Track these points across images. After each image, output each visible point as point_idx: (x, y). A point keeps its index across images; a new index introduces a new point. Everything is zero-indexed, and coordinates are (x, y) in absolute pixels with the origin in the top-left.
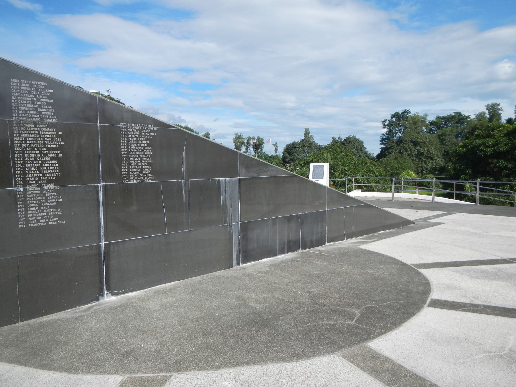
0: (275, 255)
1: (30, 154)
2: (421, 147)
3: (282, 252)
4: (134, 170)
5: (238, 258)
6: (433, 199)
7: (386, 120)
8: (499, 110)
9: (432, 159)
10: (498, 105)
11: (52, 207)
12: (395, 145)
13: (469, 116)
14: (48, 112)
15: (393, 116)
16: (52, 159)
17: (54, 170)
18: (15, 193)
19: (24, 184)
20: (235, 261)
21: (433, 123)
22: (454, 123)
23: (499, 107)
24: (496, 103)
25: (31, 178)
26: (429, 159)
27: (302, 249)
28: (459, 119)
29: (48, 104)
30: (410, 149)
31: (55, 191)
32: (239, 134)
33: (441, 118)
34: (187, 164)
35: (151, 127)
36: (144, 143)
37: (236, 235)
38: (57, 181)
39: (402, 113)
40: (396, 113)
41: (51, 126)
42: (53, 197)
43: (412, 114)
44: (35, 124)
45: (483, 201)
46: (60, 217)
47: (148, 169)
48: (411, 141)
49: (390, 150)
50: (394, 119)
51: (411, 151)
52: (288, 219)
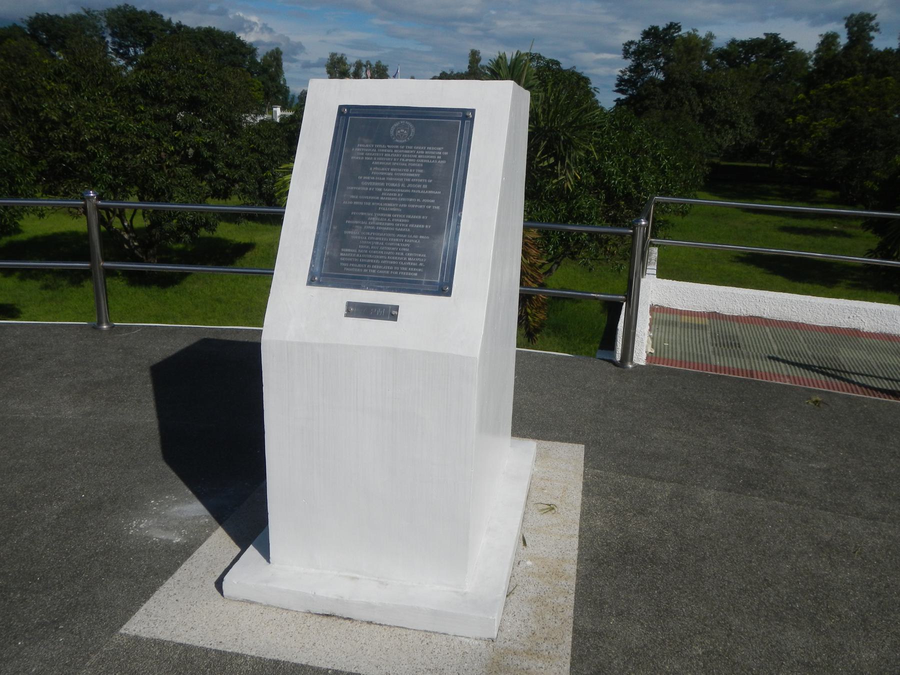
2: (713, 99)
7: (632, 43)
9: (733, 125)
10: (873, 18)
12: (659, 90)
13: (794, 43)
15: (646, 34)
21: (722, 54)
22: (763, 57)
24: (868, 15)
26: (727, 126)
28: (773, 48)
30: (689, 101)
32: (339, 56)
33: (738, 45)
39: (664, 29)
43: (684, 32)
48: (693, 84)
49: (648, 102)
50: (647, 41)
51: (691, 105)
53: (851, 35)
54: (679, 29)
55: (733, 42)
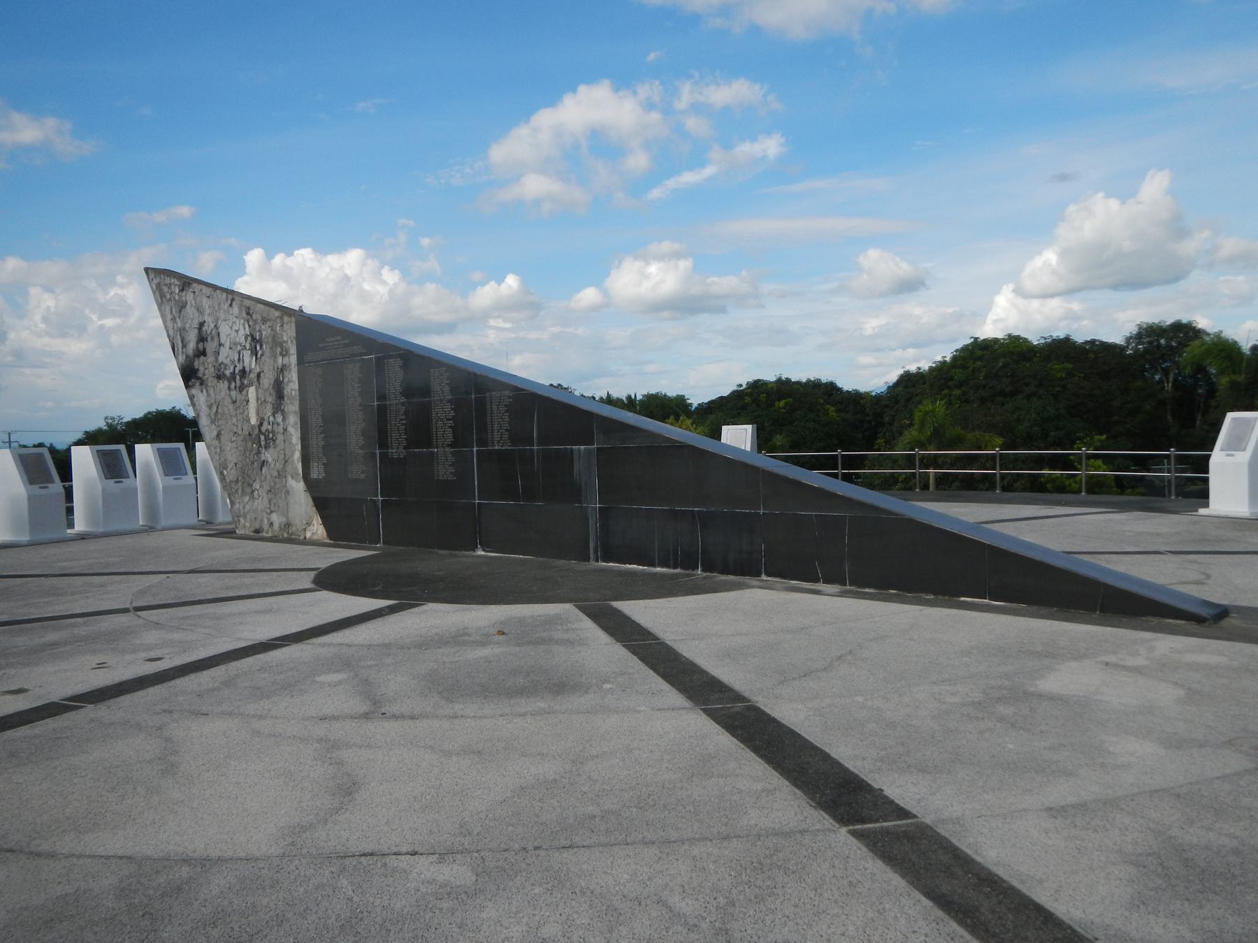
0: (653, 565)
4: (496, 436)
5: (596, 552)
20: (592, 555)
25: (440, 442)
27: (704, 570)
34: (539, 430)
36: (503, 409)
41: (449, 401)
47: (506, 436)
52: (674, 514)
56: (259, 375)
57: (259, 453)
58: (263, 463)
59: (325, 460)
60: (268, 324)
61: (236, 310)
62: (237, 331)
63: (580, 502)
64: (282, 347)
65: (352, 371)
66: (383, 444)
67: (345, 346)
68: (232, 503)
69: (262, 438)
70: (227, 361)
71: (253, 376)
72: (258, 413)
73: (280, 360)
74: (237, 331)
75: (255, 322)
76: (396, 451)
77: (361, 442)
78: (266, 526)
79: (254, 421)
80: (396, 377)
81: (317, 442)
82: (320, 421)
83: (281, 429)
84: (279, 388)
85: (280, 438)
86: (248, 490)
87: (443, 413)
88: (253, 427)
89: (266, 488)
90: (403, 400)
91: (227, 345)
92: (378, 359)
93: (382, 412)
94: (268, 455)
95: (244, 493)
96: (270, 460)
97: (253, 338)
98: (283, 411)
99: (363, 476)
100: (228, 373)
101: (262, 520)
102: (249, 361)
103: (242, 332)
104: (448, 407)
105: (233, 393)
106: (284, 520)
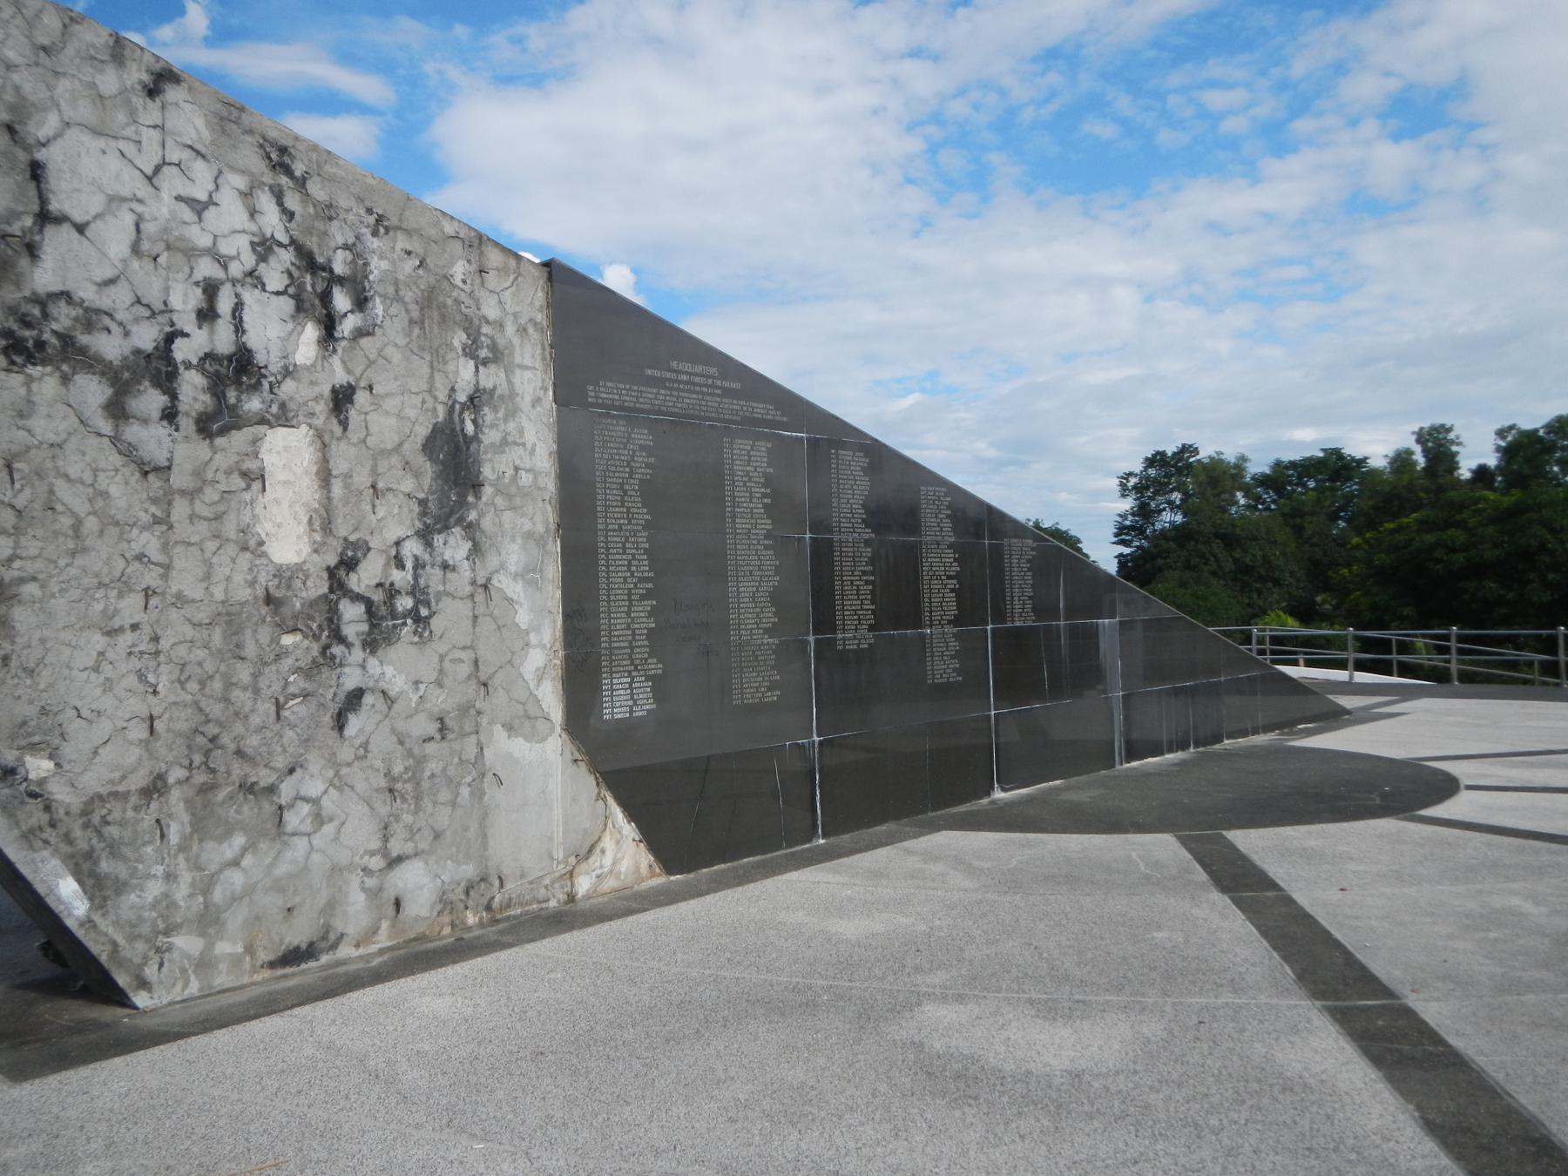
0: (1162, 754)
1: (936, 585)
3: (1171, 751)
6: (1351, 677)
7: (1131, 474)
8: (1452, 442)
9: (1277, 582)
10: (1449, 430)
11: (952, 657)
14: (947, 524)
15: (1151, 462)
16: (952, 591)
17: (952, 610)
18: (923, 636)
19: (931, 626)
21: (1264, 481)
23: (1451, 436)
24: (1443, 426)
26: (1270, 585)
28: (1336, 467)
29: (948, 516)
31: (955, 635)
33: (1286, 468)
35: (1030, 542)
37: (1119, 717)
38: (955, 622)
40: (1158, 453)
42: (954, 644)
44: (938, 544)
45: (1466, 678)
46: (958, 671)
48: (1217, 535)
49: (1160, 562)
50: (1152, 472)
51: (1217, 560)
53: (1426, 452)
54: (1196, 451)
55: (1278, 464)
56: (342, 399)
57: (327, 659)
58: (355, 698)
59: (655, 668)
60: (402, 243)
61: (188, 119)
62: (200, 208)
63: (1105, 692)
64: (472, 328)
65: (749, 462)
66: (825, 620)
67: (727, 393)
68: (97, 887)
69: (352, 616)
70: (118, 299)
71: (308, 393)
72: (324, 521)
73: (465, 374)
74: (200, 208)
75: (328, 212)
76: (854, 635)
77: (769, 617)
78: (356, 910)
79: (289, 543)
80: (853, 491)
81: (626, 620)
82: (645, 569)
83: (461, 581)
84: (454, 459)
85: (450, 618)
86: (247, 810)
87: (939, 564)
88: (285, 576)
89: (366, 780)
90: (868, 534)
91: (115, 237)
92: (814, 444)
93: (823, 553)
94: (395, 669)
95: (204, 824)
96: (397, 682)
97: (309, 261)
98: (471, 529)
99: (772, 697)
100: (111, 347)
101: (331, 907)
102: (273, 329)
103: (229, 215)
104: (949, 556)
105: (153, 439)
106: (469, 871)
